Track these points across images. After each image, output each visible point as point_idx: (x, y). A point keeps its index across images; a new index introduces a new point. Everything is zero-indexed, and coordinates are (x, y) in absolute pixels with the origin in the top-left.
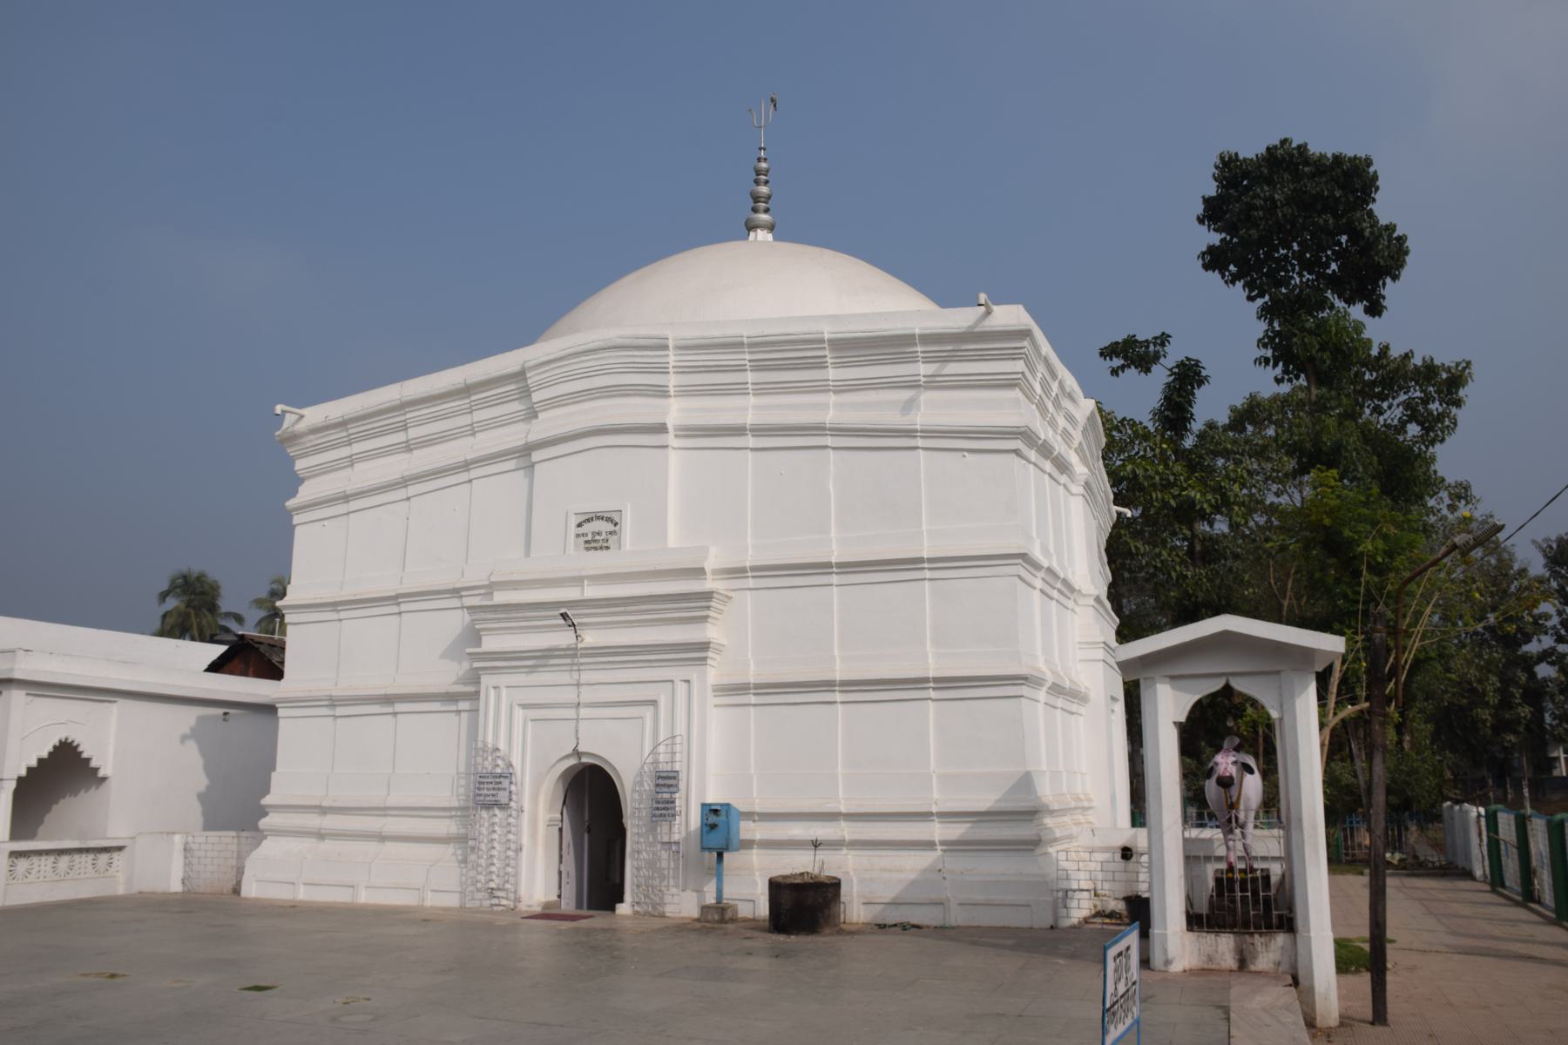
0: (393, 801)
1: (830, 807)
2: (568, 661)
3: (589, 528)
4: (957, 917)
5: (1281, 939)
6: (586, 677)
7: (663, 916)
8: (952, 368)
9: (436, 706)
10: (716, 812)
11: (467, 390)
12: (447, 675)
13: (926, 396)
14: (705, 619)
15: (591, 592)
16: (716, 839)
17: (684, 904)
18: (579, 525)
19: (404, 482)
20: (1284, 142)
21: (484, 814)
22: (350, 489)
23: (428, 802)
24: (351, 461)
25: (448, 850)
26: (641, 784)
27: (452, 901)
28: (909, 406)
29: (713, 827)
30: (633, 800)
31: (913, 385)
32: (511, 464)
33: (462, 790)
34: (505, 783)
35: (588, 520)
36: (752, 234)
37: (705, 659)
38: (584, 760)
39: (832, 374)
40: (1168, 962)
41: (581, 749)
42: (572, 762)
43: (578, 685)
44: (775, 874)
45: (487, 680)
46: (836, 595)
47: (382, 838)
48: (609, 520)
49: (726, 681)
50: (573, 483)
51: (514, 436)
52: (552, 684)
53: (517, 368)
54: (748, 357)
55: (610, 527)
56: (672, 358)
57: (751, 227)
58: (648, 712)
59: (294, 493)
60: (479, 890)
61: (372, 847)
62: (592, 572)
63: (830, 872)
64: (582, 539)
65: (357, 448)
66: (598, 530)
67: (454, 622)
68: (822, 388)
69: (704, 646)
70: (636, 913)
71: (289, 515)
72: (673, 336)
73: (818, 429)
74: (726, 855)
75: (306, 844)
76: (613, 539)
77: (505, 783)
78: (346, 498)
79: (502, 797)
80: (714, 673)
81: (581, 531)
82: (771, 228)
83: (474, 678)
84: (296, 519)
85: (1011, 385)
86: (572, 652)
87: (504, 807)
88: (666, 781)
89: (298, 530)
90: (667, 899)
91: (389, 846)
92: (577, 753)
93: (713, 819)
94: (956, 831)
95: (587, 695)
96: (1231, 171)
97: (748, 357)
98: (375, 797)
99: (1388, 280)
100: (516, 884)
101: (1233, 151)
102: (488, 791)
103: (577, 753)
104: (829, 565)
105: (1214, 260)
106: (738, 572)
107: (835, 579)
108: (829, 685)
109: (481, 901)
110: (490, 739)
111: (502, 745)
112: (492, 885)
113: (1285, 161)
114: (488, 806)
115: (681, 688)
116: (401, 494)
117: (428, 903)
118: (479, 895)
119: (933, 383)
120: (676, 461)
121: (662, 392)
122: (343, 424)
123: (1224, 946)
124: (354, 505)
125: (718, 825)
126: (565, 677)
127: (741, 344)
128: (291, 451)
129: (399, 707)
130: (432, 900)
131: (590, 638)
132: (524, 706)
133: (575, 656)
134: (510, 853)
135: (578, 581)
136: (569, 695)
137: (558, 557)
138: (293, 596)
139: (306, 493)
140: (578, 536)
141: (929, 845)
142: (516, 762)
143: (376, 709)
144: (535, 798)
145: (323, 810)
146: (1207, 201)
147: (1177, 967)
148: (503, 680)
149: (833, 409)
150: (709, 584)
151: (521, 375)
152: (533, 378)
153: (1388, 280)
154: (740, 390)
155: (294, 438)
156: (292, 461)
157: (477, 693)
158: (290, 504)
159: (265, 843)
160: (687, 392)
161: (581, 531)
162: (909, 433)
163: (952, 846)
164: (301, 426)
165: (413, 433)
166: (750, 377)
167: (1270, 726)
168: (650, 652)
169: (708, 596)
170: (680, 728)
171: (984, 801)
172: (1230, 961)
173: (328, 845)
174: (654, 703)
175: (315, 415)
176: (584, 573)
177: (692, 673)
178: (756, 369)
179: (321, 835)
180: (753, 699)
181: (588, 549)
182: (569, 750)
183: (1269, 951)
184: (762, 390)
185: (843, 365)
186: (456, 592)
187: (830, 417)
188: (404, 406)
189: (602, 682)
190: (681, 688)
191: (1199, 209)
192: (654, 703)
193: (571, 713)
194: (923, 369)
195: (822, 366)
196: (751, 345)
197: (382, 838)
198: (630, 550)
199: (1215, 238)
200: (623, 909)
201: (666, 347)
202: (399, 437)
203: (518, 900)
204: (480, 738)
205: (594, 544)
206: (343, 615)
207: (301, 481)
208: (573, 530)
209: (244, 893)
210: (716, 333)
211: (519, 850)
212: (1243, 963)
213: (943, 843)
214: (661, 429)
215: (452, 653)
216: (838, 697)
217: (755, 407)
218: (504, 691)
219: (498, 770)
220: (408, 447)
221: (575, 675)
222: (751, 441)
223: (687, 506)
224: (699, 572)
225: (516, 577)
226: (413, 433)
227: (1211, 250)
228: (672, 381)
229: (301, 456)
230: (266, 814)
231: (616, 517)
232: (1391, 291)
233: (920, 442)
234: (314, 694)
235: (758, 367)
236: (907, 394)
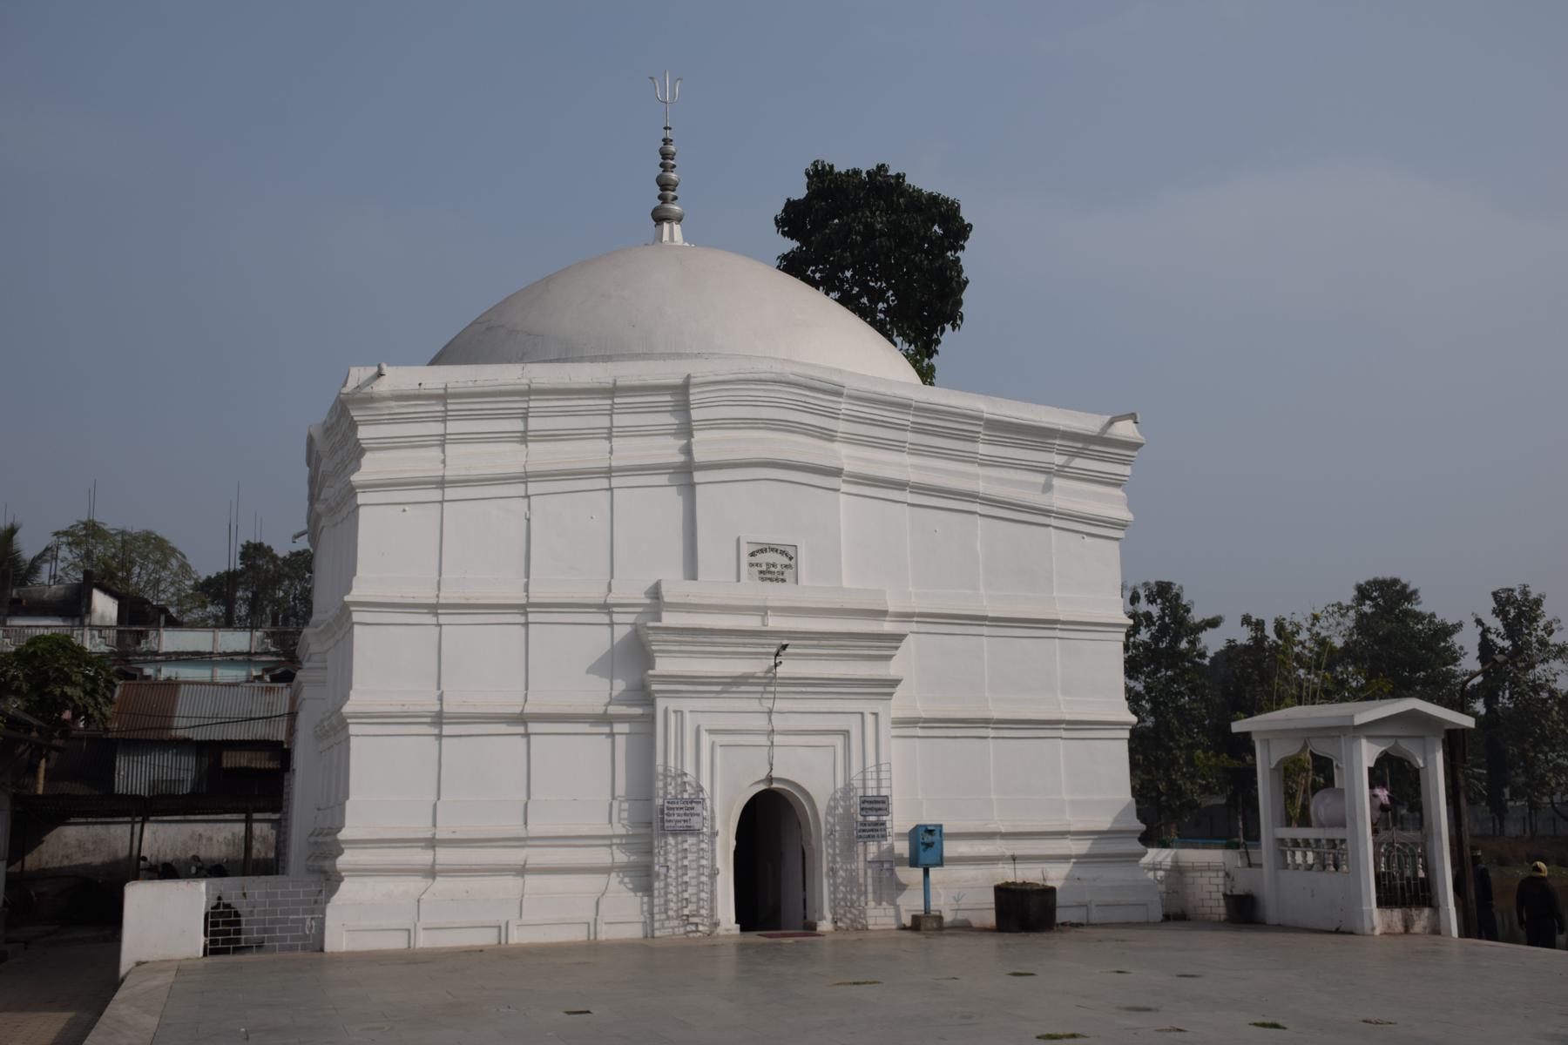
0: (535, 828)
1: (992, 827)
2: (761, 689)
3: (760, 558)
4: (1096, 916)
5: (1426, 911)
6: (780, 705)
7: (865, 928)
8: (1078, 463)
9: (585, 728)
10: (930, 832)
11: (613, 391)
12: (596, 694)
13: (1056, 482)
14: (889, 657)
15: (775, 623)
16: (925, 856)
17: (880, 917)
18: (752, 554)
19: (525, 478)
20: (882, 168)
21: (671, 840)
22: (450, 473)
23: (585, 831)
24: (443, 441)
25: (614, 879)
26: (835, 808)
27: (634, 932)
28: (1047, 488)
29: (929, 845)
30: (827, 822)
31: (1047, 471)
32: (664, 479)
33: (624, 815)
34: (698, 808)
35: (762, 551)
36: (666, 226)
37: (891, 694)
38: (775, 785)
39: (982, 449)
40: (1373, 929)
41: (774, 775)
42: (762, 787)
43: (770, 712)
44: (1000, 882)
45: (661, 704)
46: (986, 644)
47: (522, 871)
48: (783, 553)
49: (901, 714)
50: (735, 512)
51: (668, 450)
52: (743, 711)
53: (679, 381)
54: (911, 419)
55: (785, 561)
56: (844, 406)
57: (660, 218)
58: (839, 741)
59: (357, 468)
60: (668, 918)
61: (511, 883)
62: (777, 604)
63: (1049, 884)
64: (756, 569)
65: (453, 427)
66: (774, 562)
67: (597, 639)
68: (970, 459)
69: (894, 683)
70: (837, 929)
71: (352, 491)
72: (852, 385)
73: (972, 496)
74: (932, 871)
75: (415, 884)
76: (788, 574)
77: (698, 808)
78: (442, 483)
79: (695, 822)
80: (901, 704)
81: (754, 560)
82: (679, 220)
83: (648, 700)
84: (361, 498)
85: (1117, 485)
86: (769, 681)
87: (695, 832)
88: (878, 805)
89: (362, 511)
90: (870, 912)
91: (531, 880)
92: (770, 779)
93: (928, 839)
94: (1082, 847)
95: (778, 722)
96: (820, 176)
97: (911, 419)
98: (514, 827)
99: (948, 327)
100: (712, 909)
101: (828, 161)
102: (655, 820)
103: (770, 779)
104: (984, 618)
105: (792, 265)
106: (906, 616)
107: (985, 630)
108: (986, 722)
109: (668, 929)
110: (672, 763)
111: (687, 770)
112: (686, 912)
113: (883, 188)
114: (675, 833)
115: (870, 720)
116: (519, 489)
117: (602, 937)
118: (675, 923)
119: (1061, 472)
120: (847, 507)
121: (829, 436)
122: (443, 397)
123: (1396, 915)
124: (450, 493)
125: (926, 845)
126: (754, 705)
127: (908, 406)
128: (356, 414)
129: (533, 727)
130: (606, 934)
131: (787, 668)
132: (711, 732)
133: (769, 684)
134: (704, 879)
135: (763, 611)
136: (760, 722)
137: (722, 584)
138: (359, 592)
139: (371, 468)
140: (751, 565)
141: (1065, 858)
142: (705, 784)
143: (503, 728)
144: (726, 823)
145: (432, 843)
146: (790, 205)
147: (1377, 932)
148: (686, 704)
149: (983, 481)
150: (888, 627)
151: (682, 390)
152: (695, 396)
153: (948, 327)
154: (898, 446)
155: (371, 399)
156: (353, 426)
157: (652, 718)
158: (356, 478)
159: (343, 886)
160: (852, 440)
161: (754, 560)
162: (1046, 512)
163: (1083, 860)
164: (382, 387)
165: (534, 424)
166: (910, 437)
167: (1417, 771)
168: (852, 686)
169: (900, 638)
170: (871, 761)
171: (1104, 822)
172: (1399, 927)
173: (441, 883)
174: (846, 734)
175: (399, 378)
176: (769, 604)
177: (878, 706)
178: (915, 431)
179: (432, 872)
180: (920, 732)
181: (763, 579)
182: (763, 775)
183: (1422, 919)
184: (917, 451)
185: (991, 443)
186: (606, 608)
187: (981, 487)
188: (529, 392)
189: (792, 711)
190: (870, 720)
191: (779, 209)
192: (846, 734)
193: (763, 740)
194: (1059, 460)
195: (973, 440)
196: (917, 409)
197: (522, 871)
198: (808, 587)
199: (791, 245)
200: (825, 925)
201: (840, 394)
202: (518, 425)
203: (716, 924)
204: (659, 760)
205: (768, 575)
206: (443, 619)
207: (362, 452)
208: (745, 559)
209: (328, 947)
210: (882, 389)
211: (714, 874)
212: (1407, 929)
213: (1077, 857)
214: (836, 472)
215: (606, 666)
216: (991, 733)
217: (914, 467)
218: (688, 716)
219: (686, 796)
220: (524, 438)
221: (768, 704)
222: (909, 497)
223: (861, 552)
224: (882, 614)
225: (693, 600)
226: (534, 424)
227: (785, 257)
228: (841, 426)
229: (366, 423)
230: (340, 852)
231: (791, 552)
232: (949, 339)
233: (1053, 522)
234: (413, 709)
235: (918, 429)
236: (1041, 478)
